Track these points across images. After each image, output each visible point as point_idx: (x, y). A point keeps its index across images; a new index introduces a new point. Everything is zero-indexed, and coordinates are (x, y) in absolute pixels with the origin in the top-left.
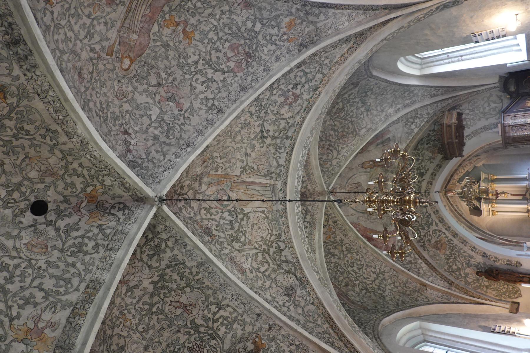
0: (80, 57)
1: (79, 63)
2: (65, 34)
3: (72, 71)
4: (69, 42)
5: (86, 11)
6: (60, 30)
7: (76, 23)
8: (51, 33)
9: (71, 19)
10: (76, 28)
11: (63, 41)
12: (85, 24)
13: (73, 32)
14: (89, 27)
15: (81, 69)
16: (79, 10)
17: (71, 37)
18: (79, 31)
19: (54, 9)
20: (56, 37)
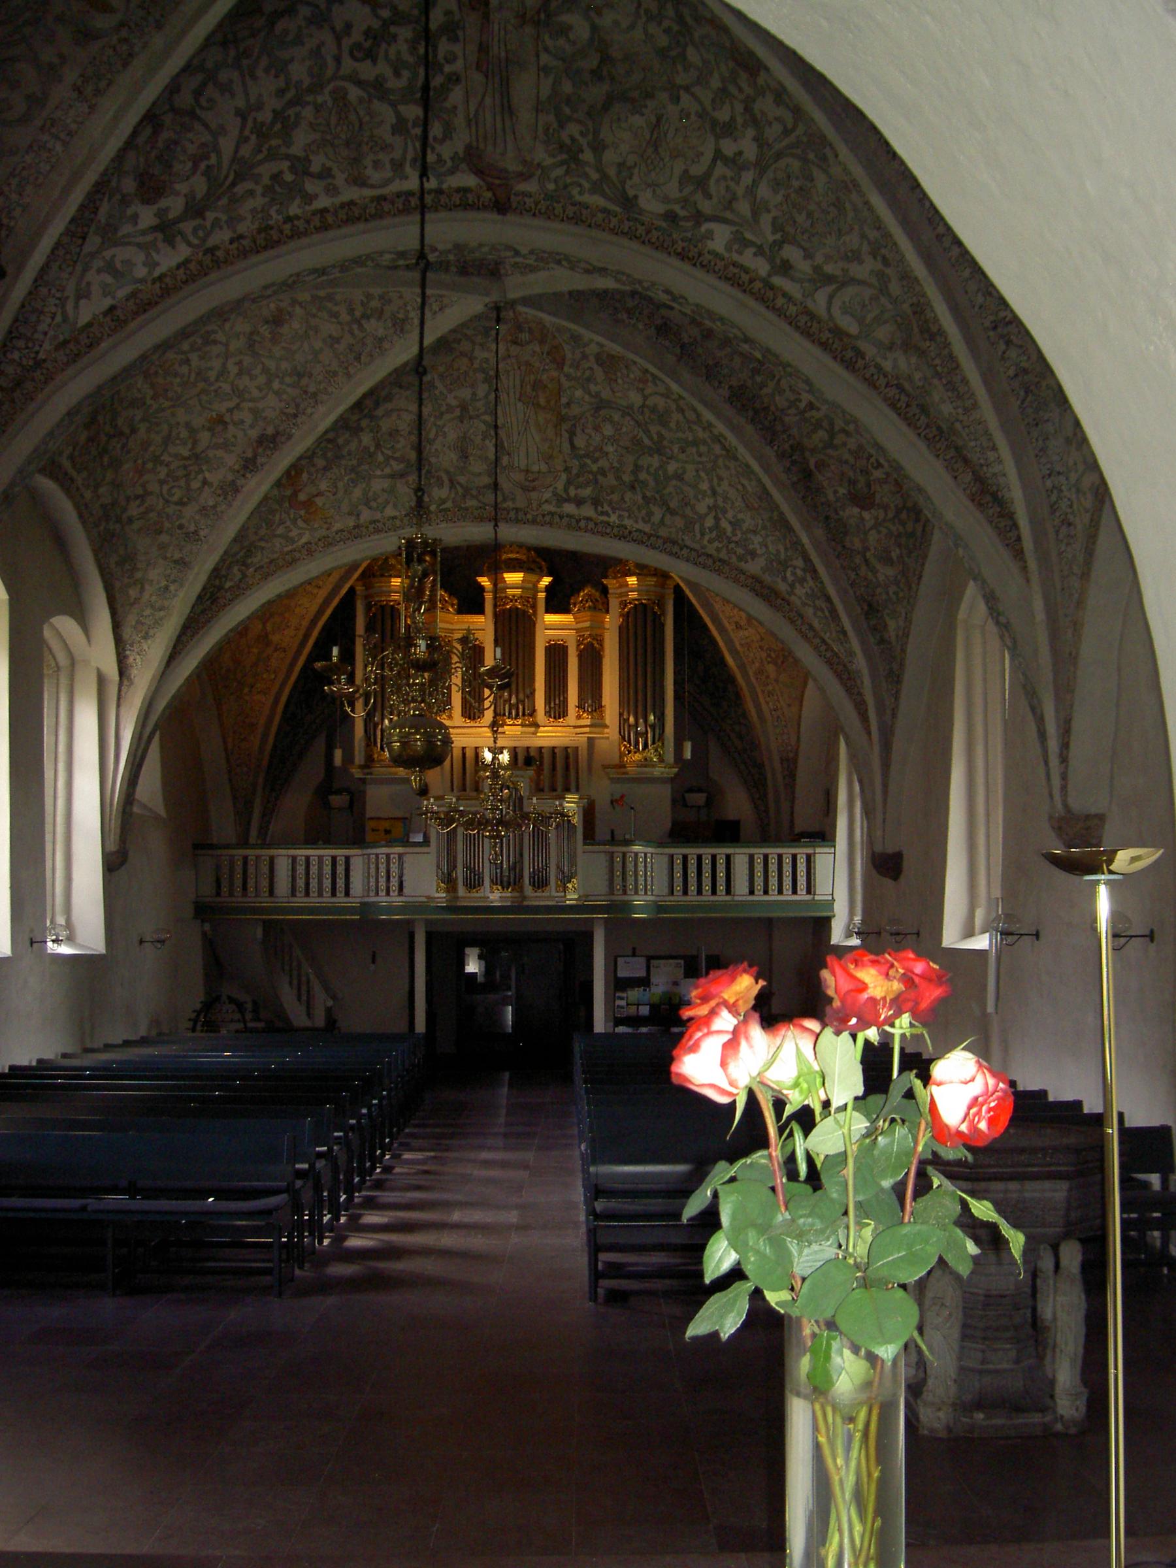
0: (252, 333)
1: (261, 330)
2: (240, 374)
3: (283, 344)
4: (245, 364)
5: (184, 369)
6: (241, 388)
7: (211, 369)
8: (260, 405)
9: (212, 379)
10: (217, 364)
11: (253, 378)
12: (201, 358)
13: (224, 365)
14: (199, 349)
15: (267, 322)
16: (192, 379)
17: (236, 364)
18: (218, 356)
19: (223, 410)
20: (256, 393)
